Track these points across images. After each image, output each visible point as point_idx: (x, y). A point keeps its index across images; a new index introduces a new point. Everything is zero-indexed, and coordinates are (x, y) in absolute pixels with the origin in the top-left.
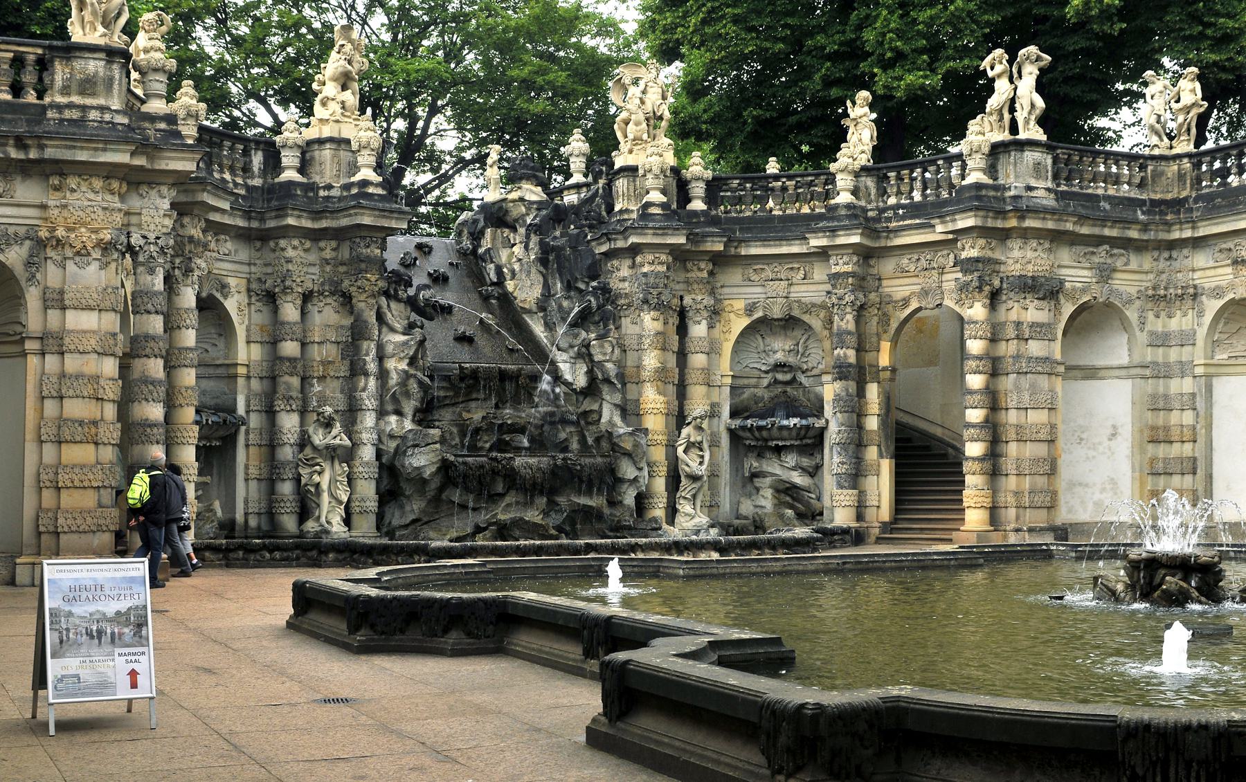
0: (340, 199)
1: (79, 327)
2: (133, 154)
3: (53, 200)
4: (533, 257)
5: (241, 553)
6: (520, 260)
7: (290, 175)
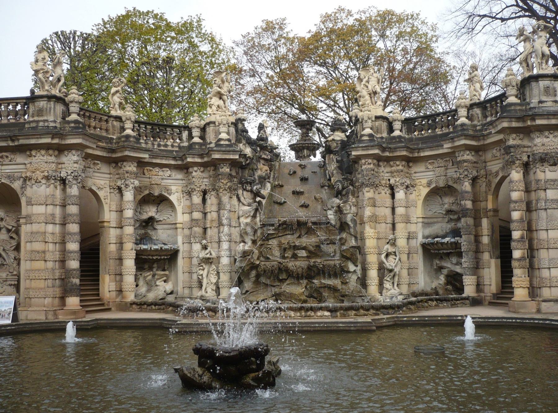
1: (38, 212)
2: (53, 138)
5: (146, 306)
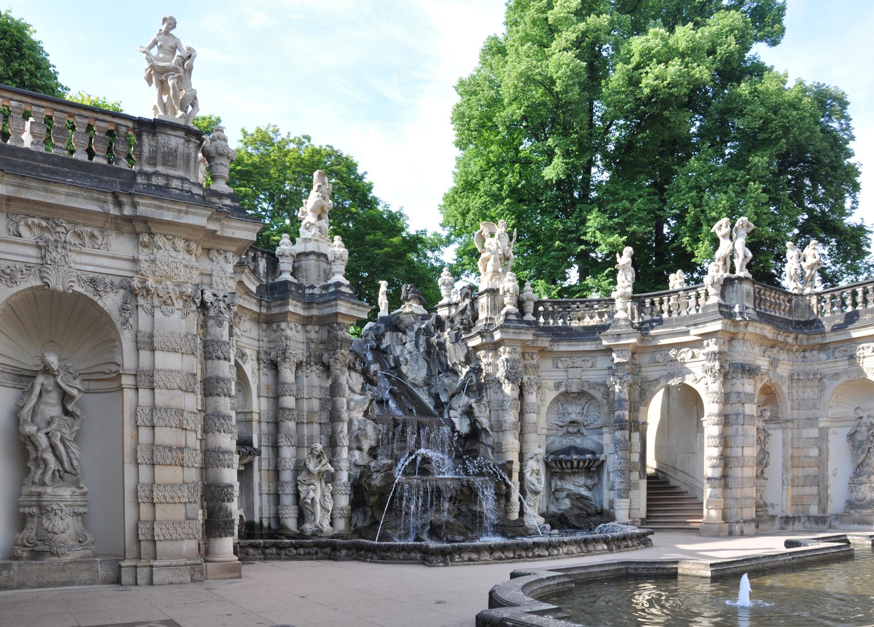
0: (321, 296)
1: (166, 367)
3: (143, 255)
4: (422, 350)
6: (410, 353)
7: (287, 276)
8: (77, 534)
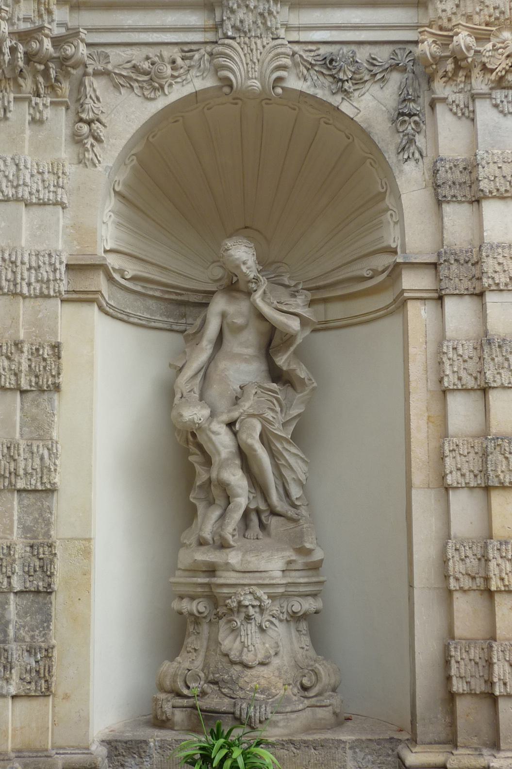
8: (297, 666)
